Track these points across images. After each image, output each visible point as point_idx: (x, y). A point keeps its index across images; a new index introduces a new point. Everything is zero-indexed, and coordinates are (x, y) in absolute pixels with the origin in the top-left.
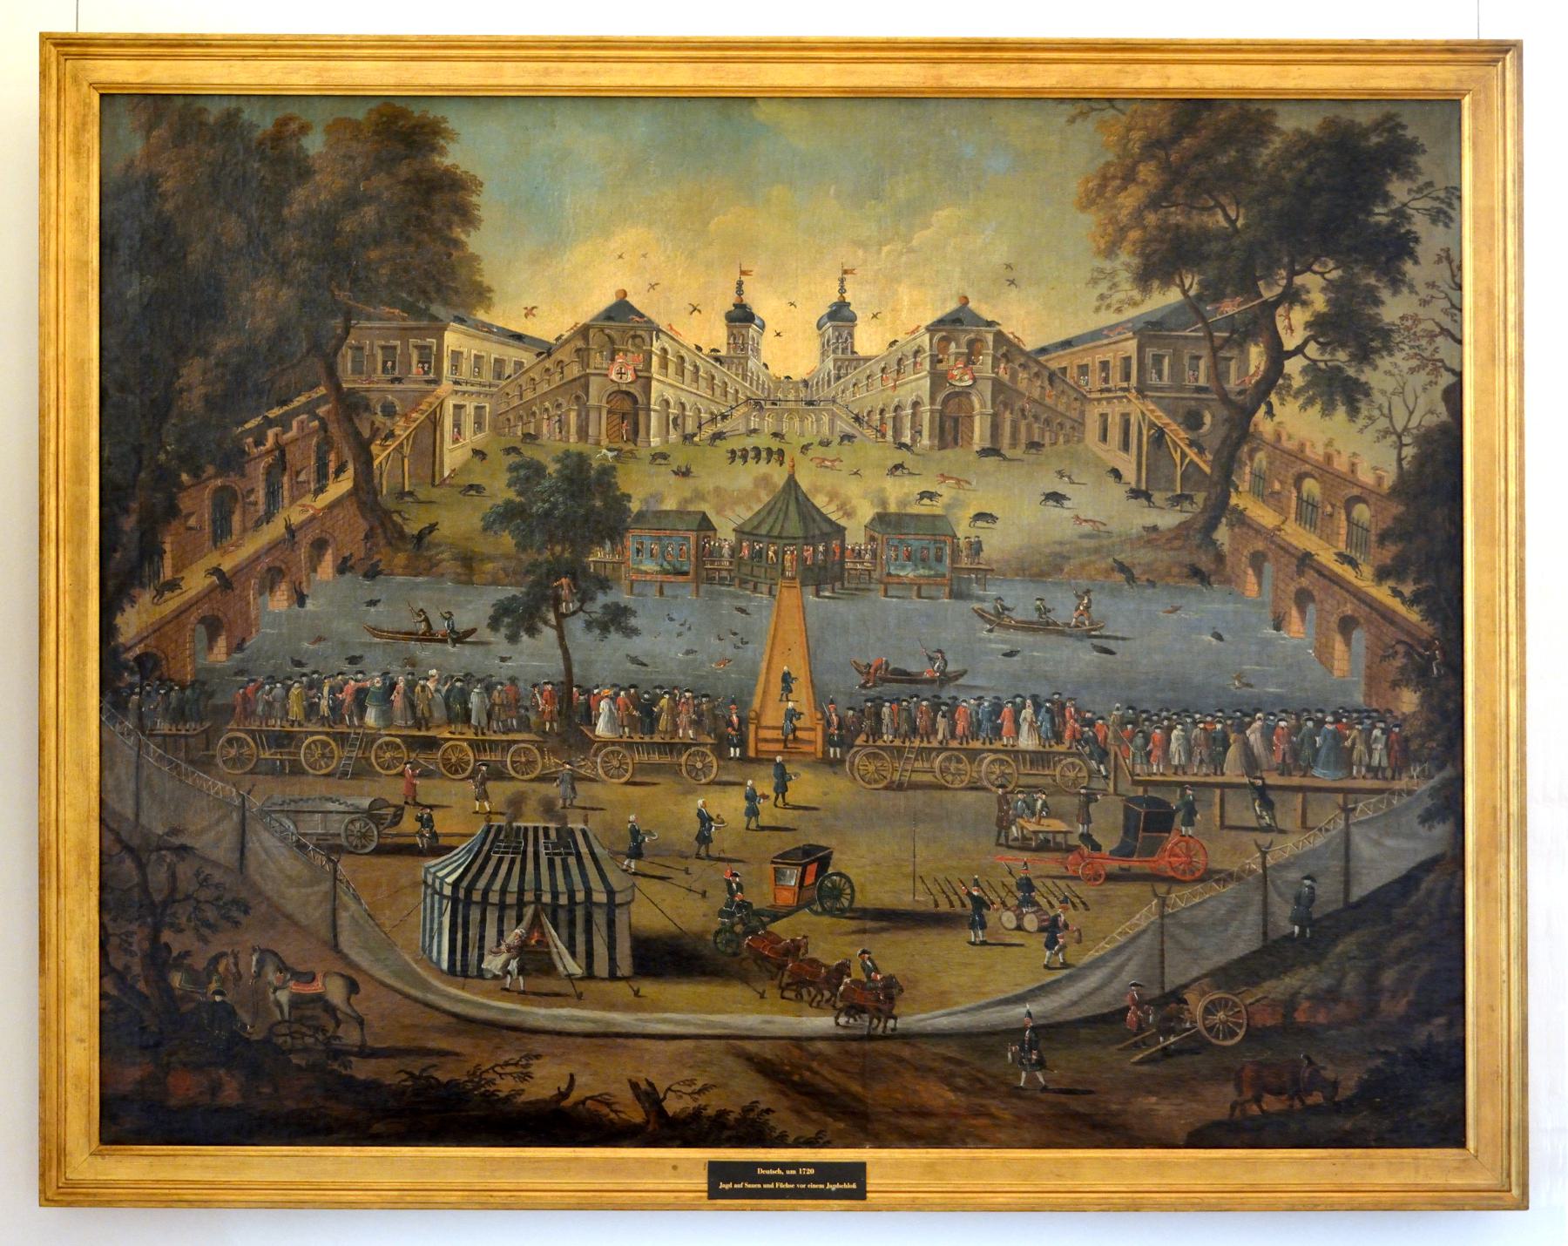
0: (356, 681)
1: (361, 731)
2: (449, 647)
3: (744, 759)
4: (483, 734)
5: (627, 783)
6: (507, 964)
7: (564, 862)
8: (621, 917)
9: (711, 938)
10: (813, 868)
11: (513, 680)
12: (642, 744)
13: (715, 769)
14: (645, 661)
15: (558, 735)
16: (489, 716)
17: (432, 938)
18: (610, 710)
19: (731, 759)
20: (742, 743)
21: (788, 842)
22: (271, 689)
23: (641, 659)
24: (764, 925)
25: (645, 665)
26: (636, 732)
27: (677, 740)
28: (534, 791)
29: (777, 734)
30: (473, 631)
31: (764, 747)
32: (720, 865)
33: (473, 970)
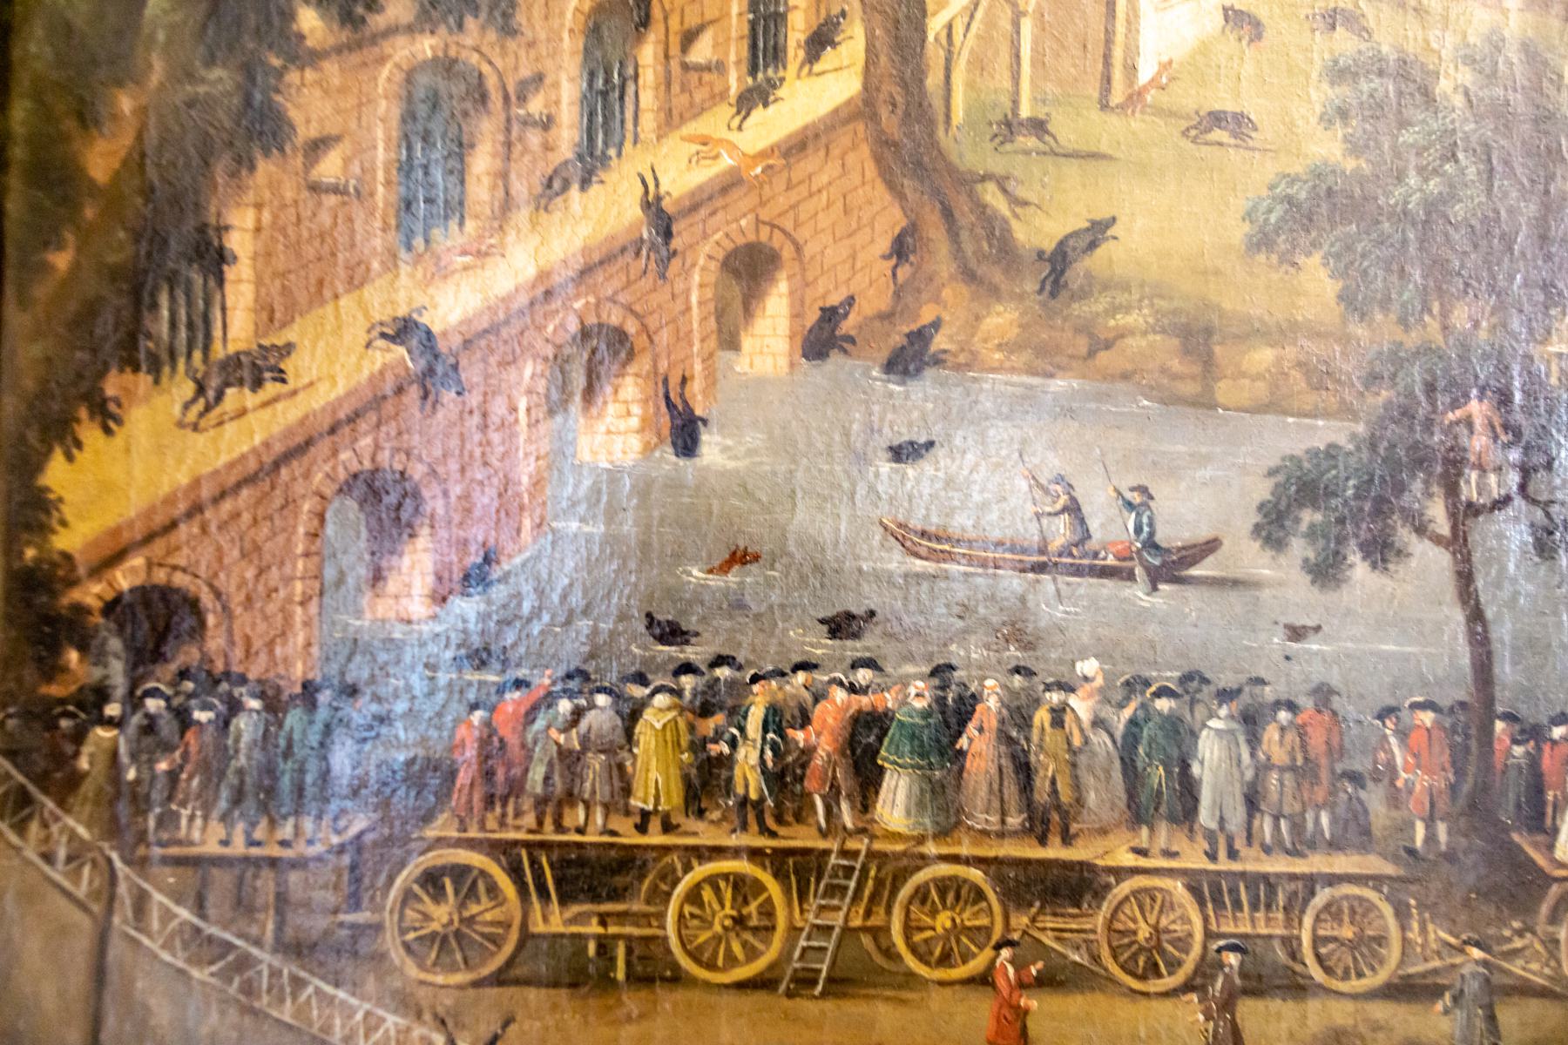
0: (852, 689)
1: (860, 845)
2: (1137, 592)
4: (1233, 854)
11: (1323, 694)
16: (1252, 802)
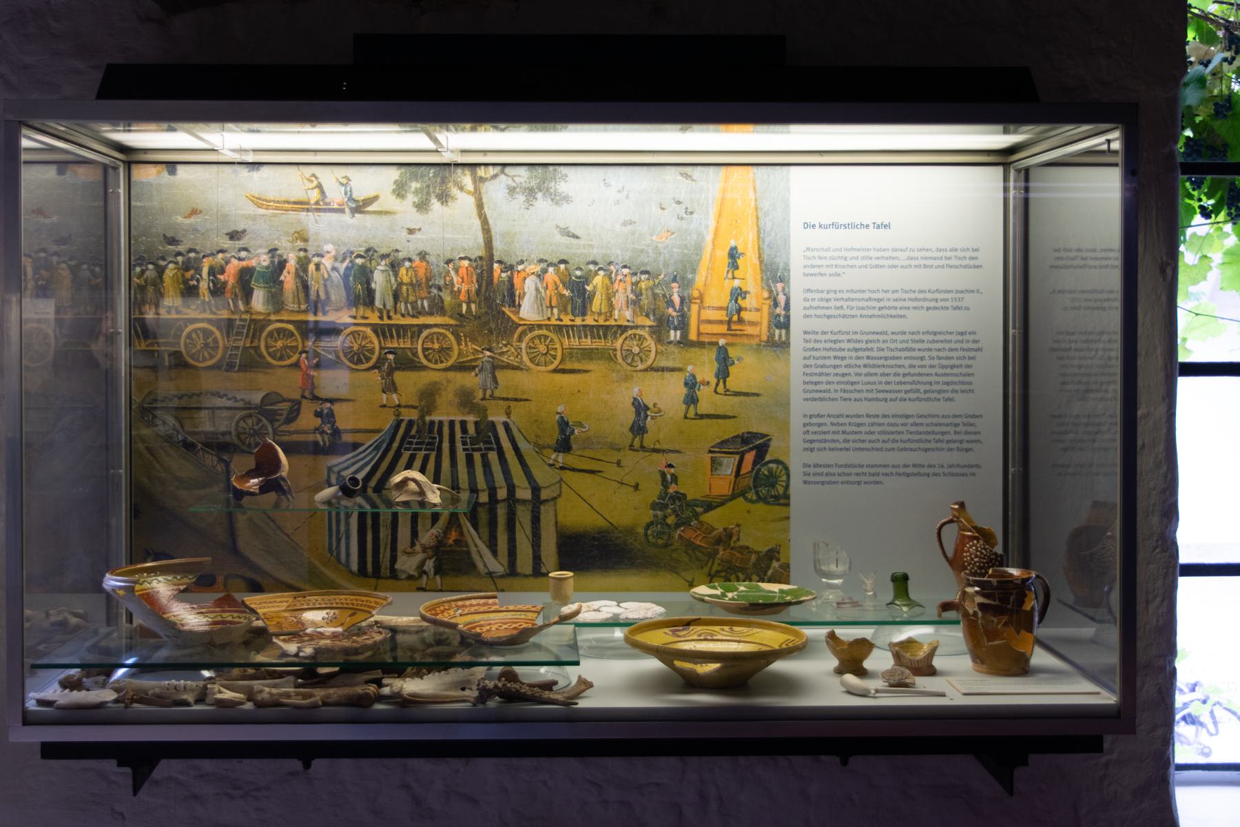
0: (240, 259)
3: (685, 343)
4: (389, 318)
5: (556, 371)
6: (423, 563)
7: (484, 457)
8: (546, 513)
9: (641, 530)
10: (750, 457)
11: (423, 256)
12: (572, 326)
13: (653, 355)
14: (577, 233)
15: (477, 317)
16: (396, 296)
17: (339, 540)
18: (537, 289)
19: (670, 343)
20: (683, 325)
21: (728, 430)
22: (143, 272)
23: (572, 230)
24: (697, 515)
25: (577, 237)
26: (567, 314)
27: (612, 322)
28: (449, 381)
29: (721, 315)
30: (376, 198)
31: (706, 328)
32: (655, 456)
33: (385, 570)
